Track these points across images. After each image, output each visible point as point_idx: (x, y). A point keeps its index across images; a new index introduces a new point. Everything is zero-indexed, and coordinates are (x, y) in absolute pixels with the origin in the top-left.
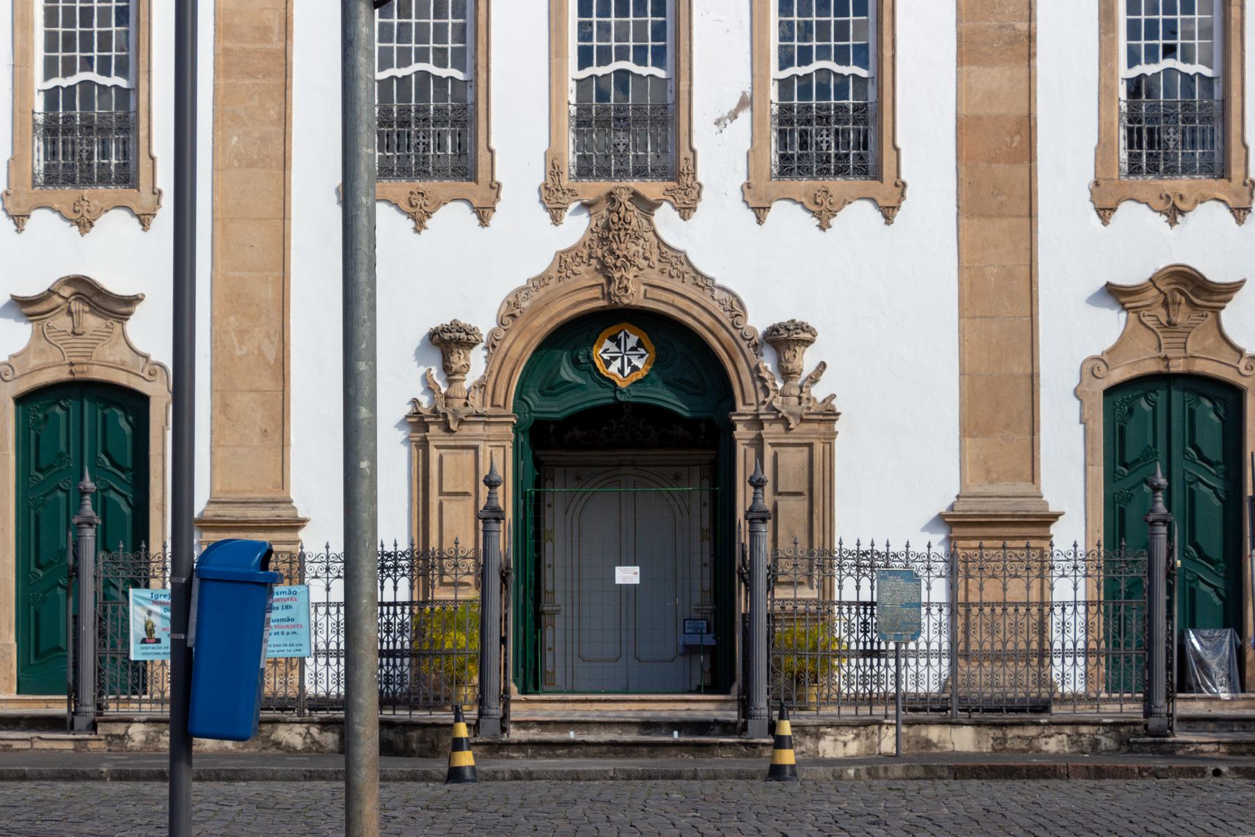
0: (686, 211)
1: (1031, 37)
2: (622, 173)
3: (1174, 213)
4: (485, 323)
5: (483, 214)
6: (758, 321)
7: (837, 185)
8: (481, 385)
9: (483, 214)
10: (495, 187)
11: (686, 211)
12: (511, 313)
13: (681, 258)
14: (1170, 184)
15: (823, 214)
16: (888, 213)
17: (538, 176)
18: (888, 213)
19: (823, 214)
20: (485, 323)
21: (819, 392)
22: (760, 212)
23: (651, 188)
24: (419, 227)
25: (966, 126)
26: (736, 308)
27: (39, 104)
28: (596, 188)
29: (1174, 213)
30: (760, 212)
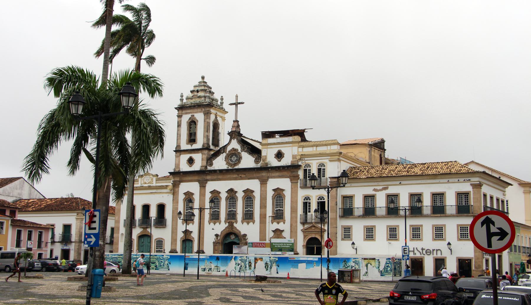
0: (236, 223)
1: (266, 206)
2: (232, 219)
3: (278, 223)
4: (219, 234)
5: (220, 223)
6: (242, 233)
7: (249, 220)
8: (219, 240)
9: (220, 223)
10: (221, 221)
11: (236, 223)
12: (221, 233)
13: (236, 227)
14: (278, 220)
15: (248, 224)
16: (254, 223)
17: (224, 220)
18: (254, 223)
19: (248, 224)
20: (219, 234)
21: (247, 241)
22: (243, 223)
23: (233, 221)
24: (215, 225)
25: (260, 215)
26: (240, 232)
27: (186, 214)
28: (228, 221)
29: (278, 223)
30: (243, 223)
